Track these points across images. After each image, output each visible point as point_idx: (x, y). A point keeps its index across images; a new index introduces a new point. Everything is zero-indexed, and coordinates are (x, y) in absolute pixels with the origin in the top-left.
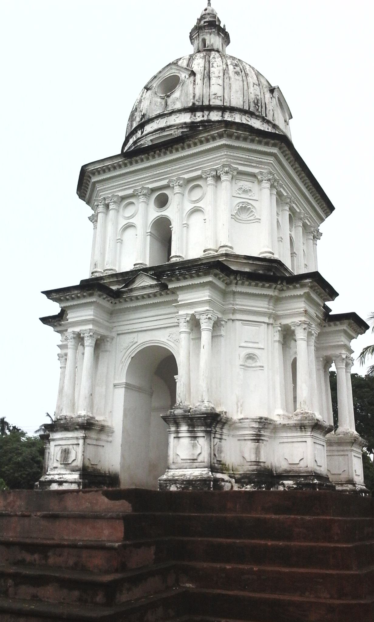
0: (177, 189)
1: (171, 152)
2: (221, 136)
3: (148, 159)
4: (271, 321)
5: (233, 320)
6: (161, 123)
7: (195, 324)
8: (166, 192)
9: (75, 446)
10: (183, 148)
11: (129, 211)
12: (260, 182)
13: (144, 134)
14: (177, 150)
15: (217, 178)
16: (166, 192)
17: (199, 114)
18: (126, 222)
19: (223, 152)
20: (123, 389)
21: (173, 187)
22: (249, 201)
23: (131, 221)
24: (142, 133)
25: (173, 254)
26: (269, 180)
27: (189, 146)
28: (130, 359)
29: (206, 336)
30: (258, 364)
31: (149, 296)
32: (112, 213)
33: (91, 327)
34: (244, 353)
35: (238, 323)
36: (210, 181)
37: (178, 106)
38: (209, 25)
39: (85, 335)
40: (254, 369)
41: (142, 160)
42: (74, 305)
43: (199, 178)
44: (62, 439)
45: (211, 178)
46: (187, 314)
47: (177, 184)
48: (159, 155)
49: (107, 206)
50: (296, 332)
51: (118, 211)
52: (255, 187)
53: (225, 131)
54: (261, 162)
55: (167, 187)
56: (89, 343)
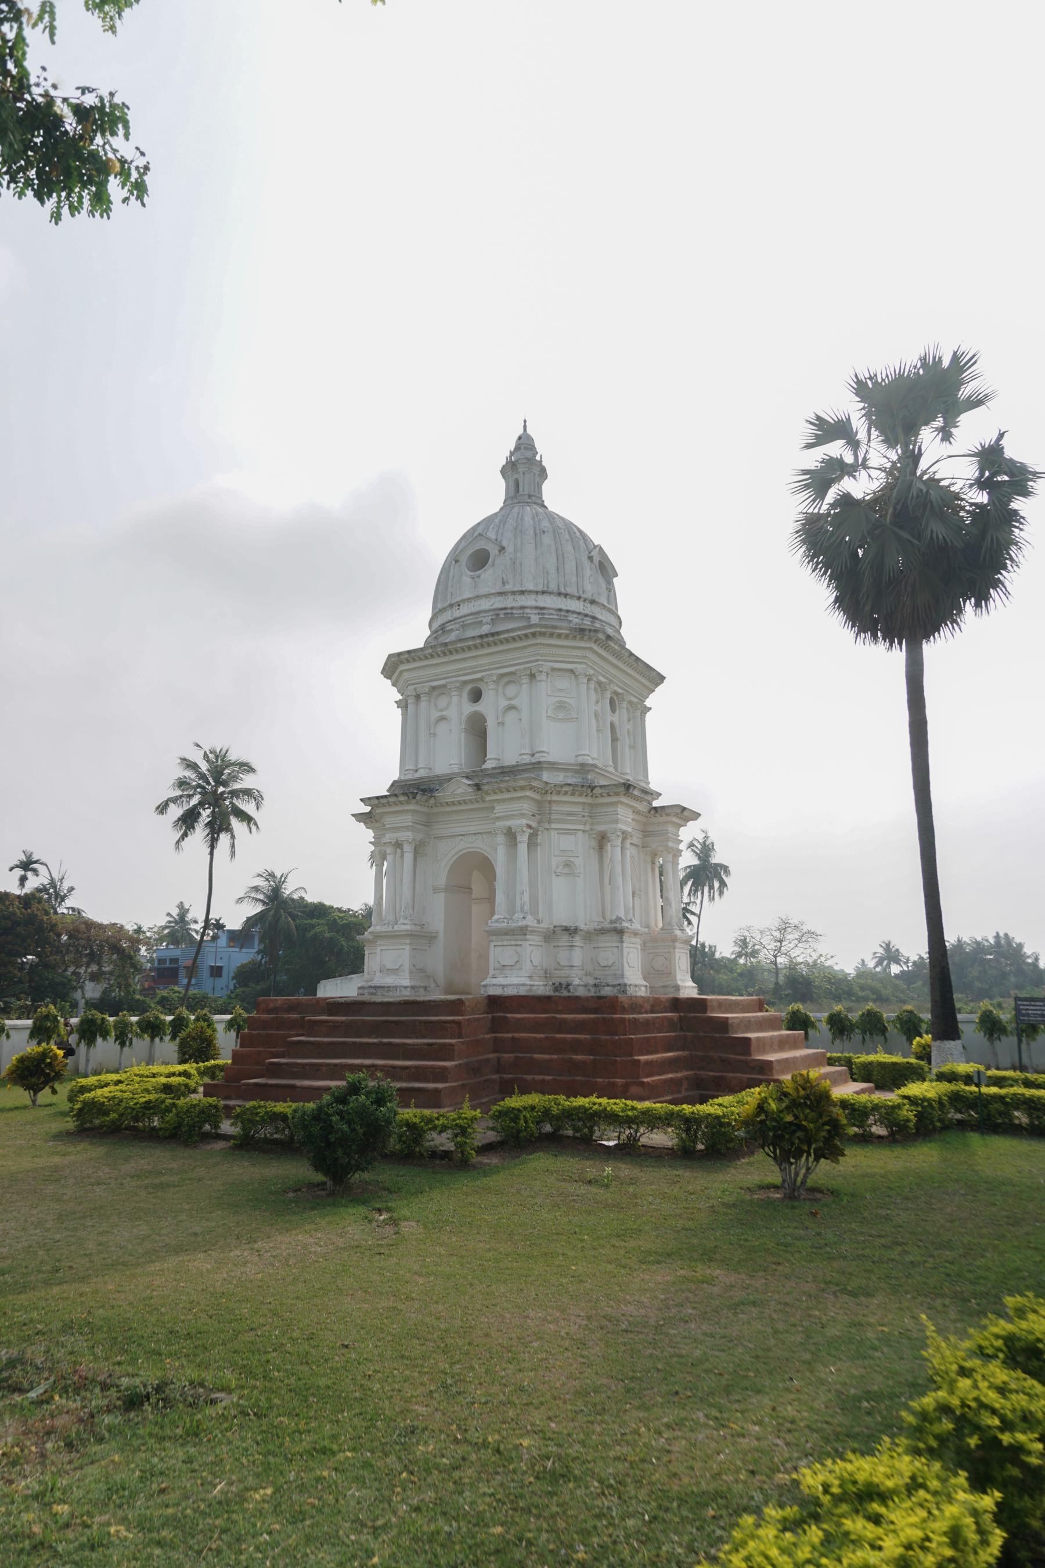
4: (588, 828)
7: (511, 835)
12: (576, 676)
15: (532, 676)
16: (480, 685)
18: (440, 714)
23: (444, 713)
25: (489, 756)
29: (523, 848)
32: (423, 704)
33: (409, 833)
36: (525, 680)
49: (418, 697)
51: (430, 701)
55: (481, 680)
56: (408, 848)
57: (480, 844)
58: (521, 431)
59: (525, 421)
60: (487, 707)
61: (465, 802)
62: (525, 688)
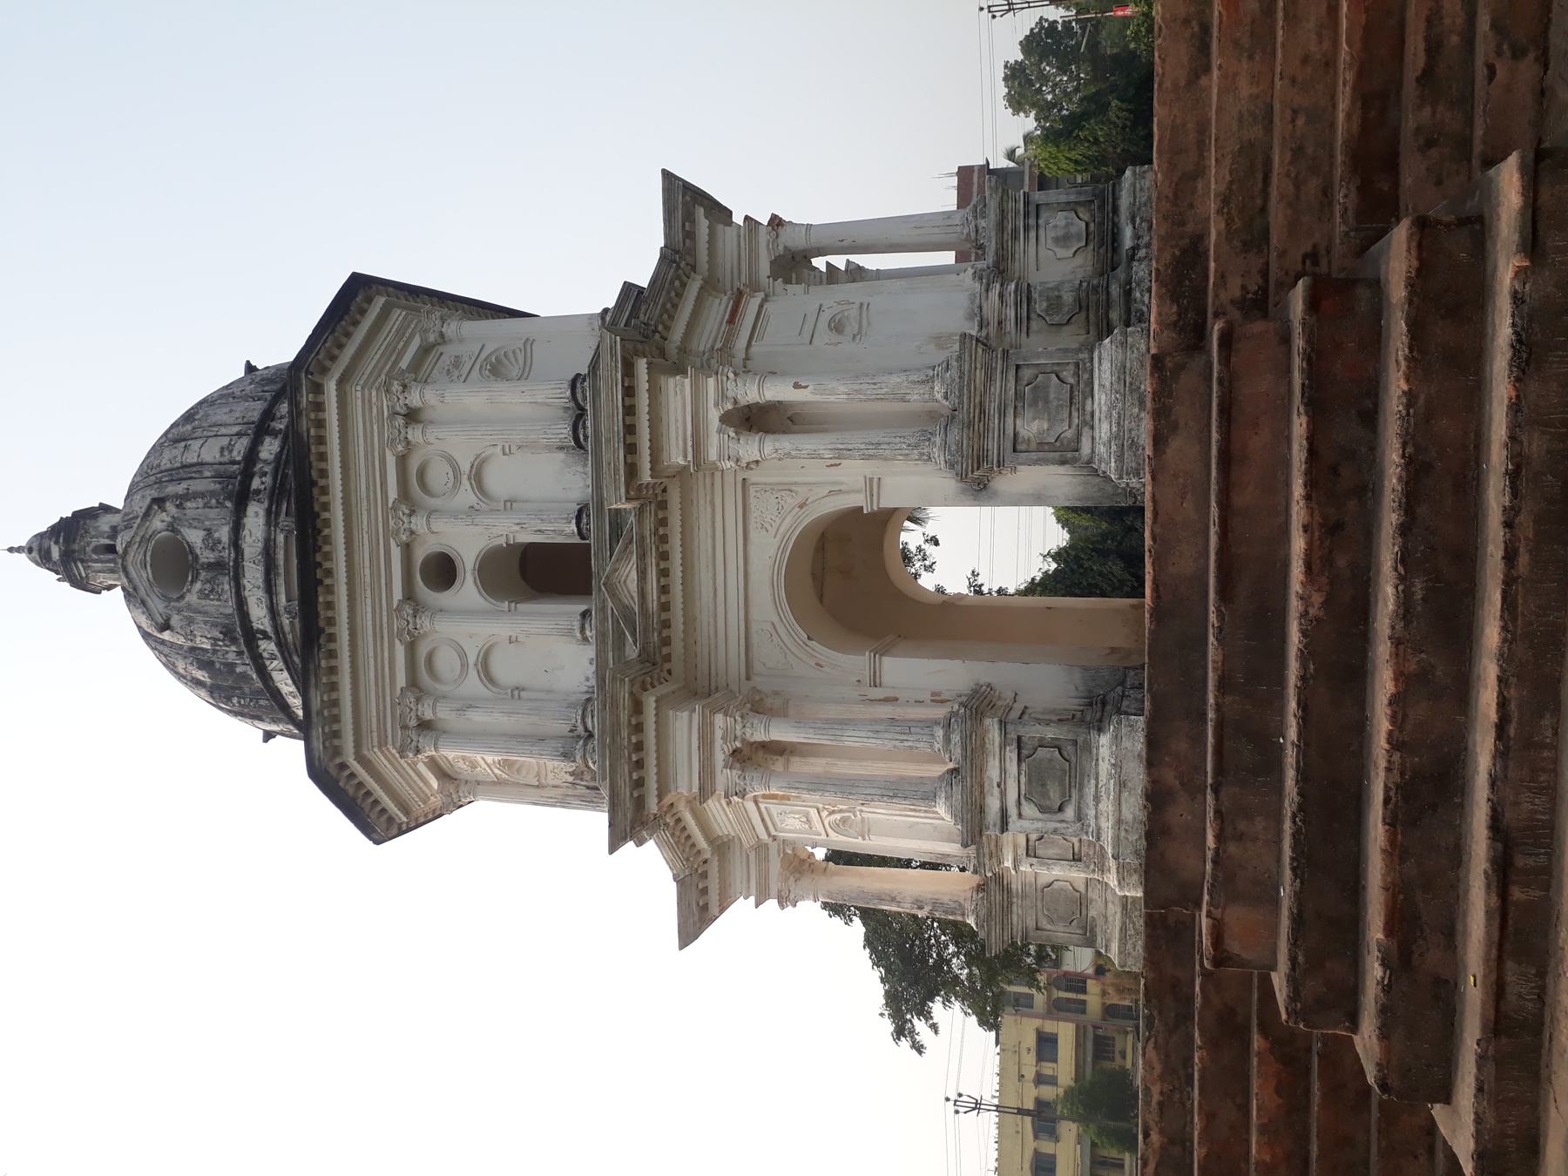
0: (418, 523)
1: (327, 523)
2: (318, 389)
3: (330, 590)
5: (747, 358)
6: (253, 575)
8: (420, 555)
9: (1025, 752)
10: (325, 491)
11: (446, 662)
13: (269, 630)
14: (326, 507)
15: (412, 416)
17: (256, 483)
18: (473, 673)
19: (356, 395)
20: (885, 659)
21: (412, 533)
22: (483, 356)
23: (472, 659)
24: (266, 636)
26: (443, 320)
27: (324, 473)
28: (813, 643)
30: (854, 312)
31: (664, 573)
32: (444, 713)
34: (824, 336)
35: (753, 349)
36: (414, 434)
37: (224, 533)
38: (71, 548)
39: (739, 733)
40: (865, 323)
41: (330, 606)
42: (658, 765)
43: (402, 461)
44: (1003, 794)
45: (410, 430)
46: (719, 431)
47: (405, 519)
48: (328, 556)
50: (790, 244)
52: (449, 351)
53: (307, 372)
54: (398, 331)
58: (24, 556)
59: (11, 550)
61: (664, 573)
62: (433, 433)
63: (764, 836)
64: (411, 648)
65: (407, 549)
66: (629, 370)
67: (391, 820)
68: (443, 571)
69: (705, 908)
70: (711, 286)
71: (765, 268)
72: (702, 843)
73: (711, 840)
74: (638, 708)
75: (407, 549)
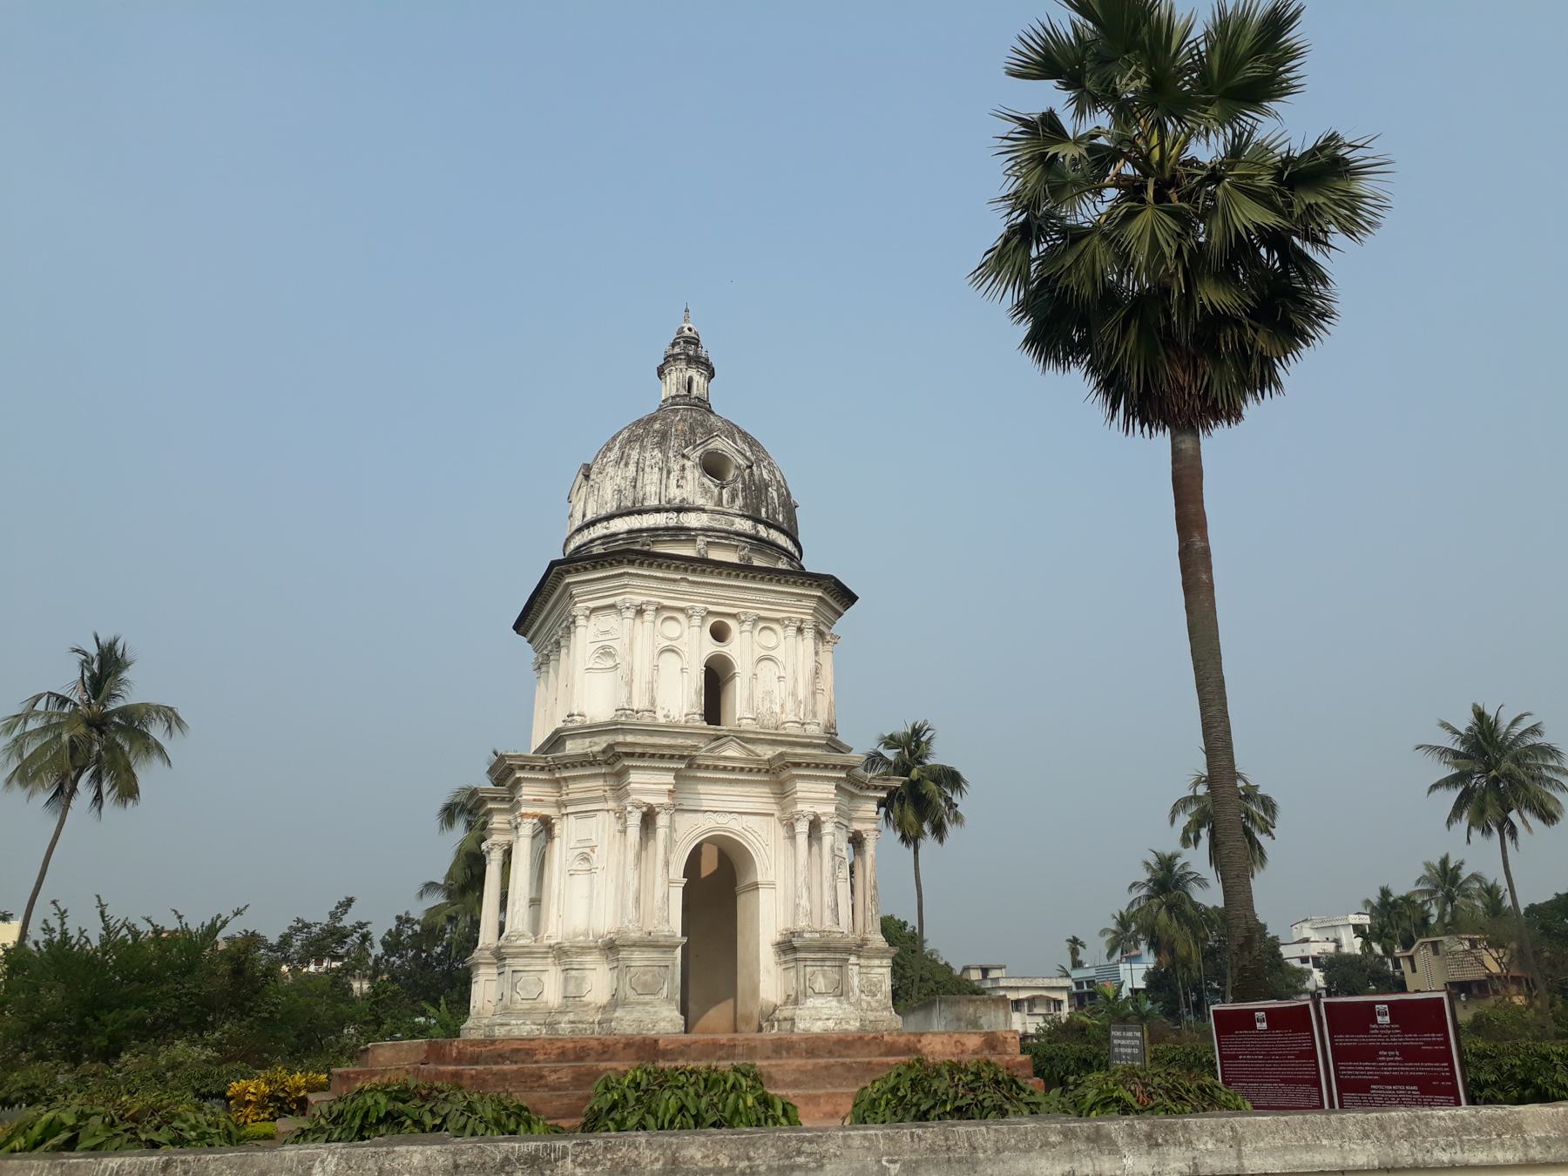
17: (761, 527)
18: (667, 643)
36: (792, 631)
49: (640, 612)
57: (735, 827)
60: (739, 648)
61: (734, 769)
63: (570, 809)
64: (681, 610)
65: (734, 616)
66: (843, 767)
67: (568, 572)
68: (719, 633)
69: (522, 768)
70: (852, 796)
71: (857, 826)
72: (566, 774)
73: (565, 779)
74: (682, 757)
75: (734, 616)
